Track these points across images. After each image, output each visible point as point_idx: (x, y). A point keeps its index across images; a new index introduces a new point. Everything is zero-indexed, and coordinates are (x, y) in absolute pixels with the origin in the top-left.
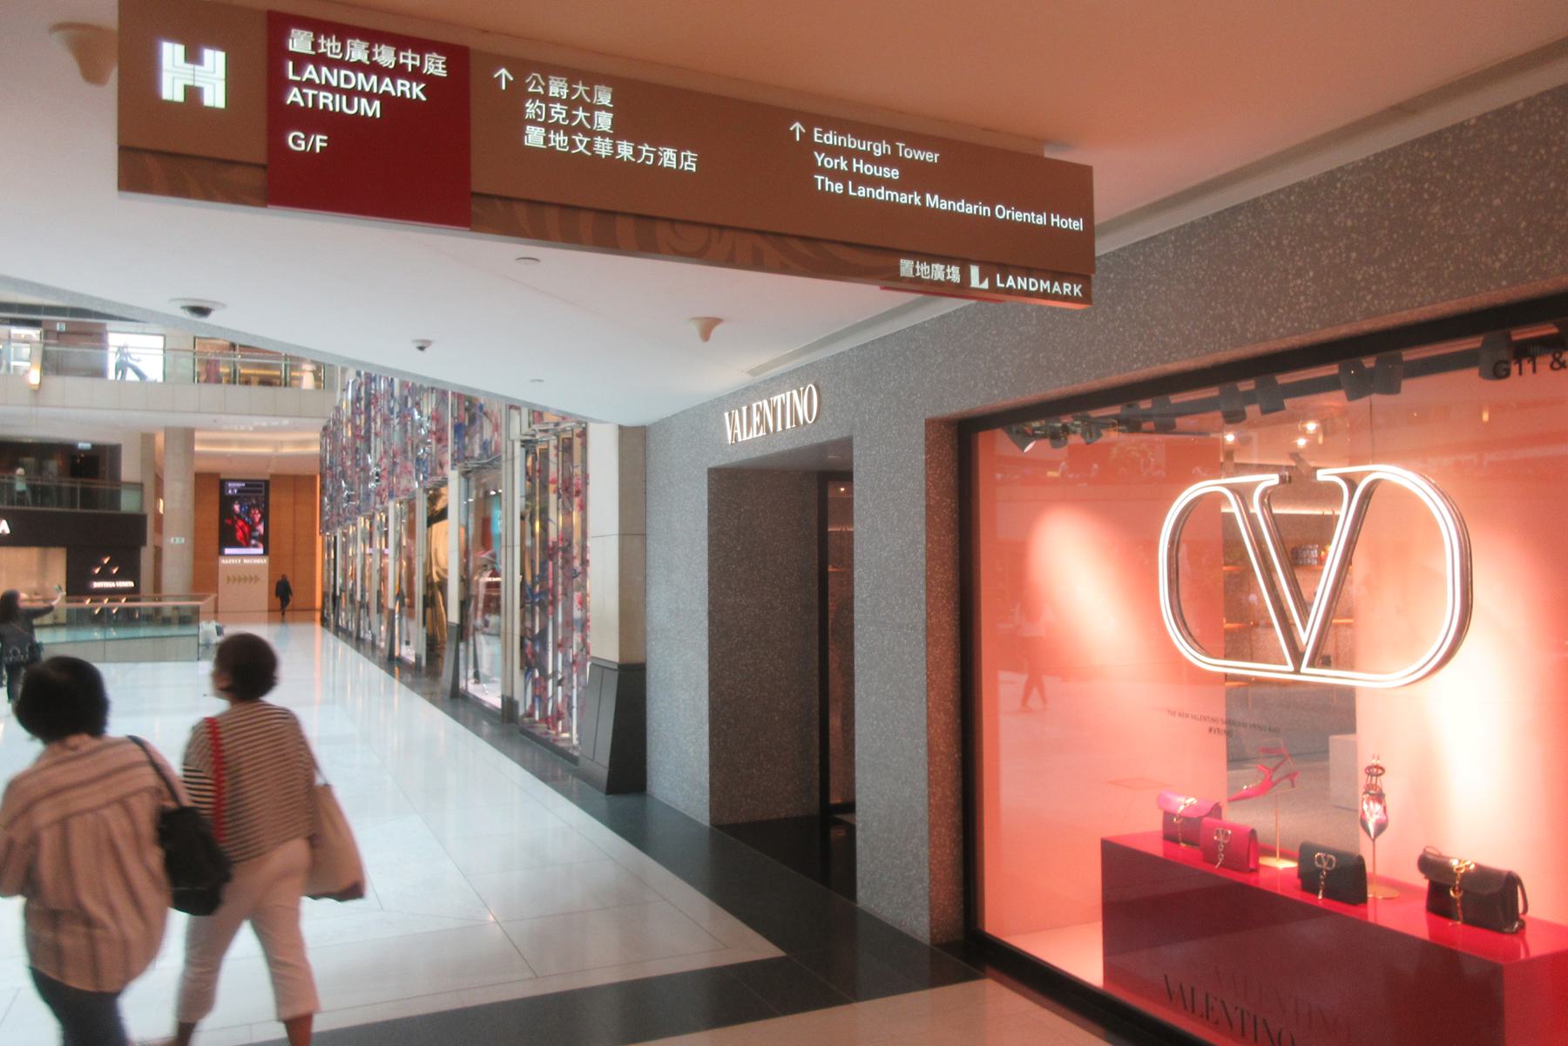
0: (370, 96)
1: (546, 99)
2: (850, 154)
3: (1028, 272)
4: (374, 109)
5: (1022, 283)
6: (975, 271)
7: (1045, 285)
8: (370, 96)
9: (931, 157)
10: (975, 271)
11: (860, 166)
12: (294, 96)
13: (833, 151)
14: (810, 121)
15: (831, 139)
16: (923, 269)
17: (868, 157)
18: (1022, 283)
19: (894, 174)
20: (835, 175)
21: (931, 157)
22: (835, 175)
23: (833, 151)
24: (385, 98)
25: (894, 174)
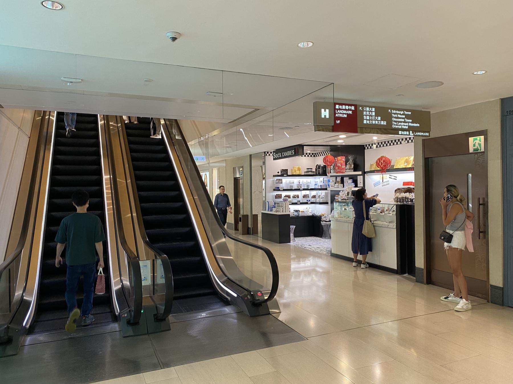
0: (345, 114)
1: (366, 111)
2: (397, 114)
3: (419, 132)
4: (345, 116)
5: (419, 134)
6: (411, 132)
7: (422, 134)
8: (345, 114)
9: (410, 113)
10: (411, 132)
11: (400, 116)
12: (337, 115)
13: (395, 114)
14: (391, 109)
15: (395, 112)
16: (403, 132)
17: (400, 114)
18: (419, 134)
19: (404, 116)
20: (395, 118)
21: (410, 113)
22: (395, 118)
23: (395, 114)
24: (347, 114)
25: (404, 116)
